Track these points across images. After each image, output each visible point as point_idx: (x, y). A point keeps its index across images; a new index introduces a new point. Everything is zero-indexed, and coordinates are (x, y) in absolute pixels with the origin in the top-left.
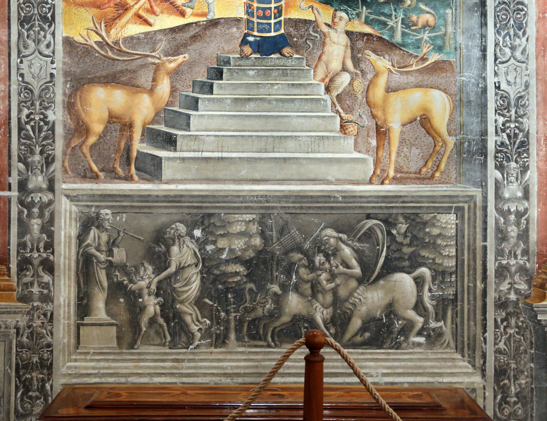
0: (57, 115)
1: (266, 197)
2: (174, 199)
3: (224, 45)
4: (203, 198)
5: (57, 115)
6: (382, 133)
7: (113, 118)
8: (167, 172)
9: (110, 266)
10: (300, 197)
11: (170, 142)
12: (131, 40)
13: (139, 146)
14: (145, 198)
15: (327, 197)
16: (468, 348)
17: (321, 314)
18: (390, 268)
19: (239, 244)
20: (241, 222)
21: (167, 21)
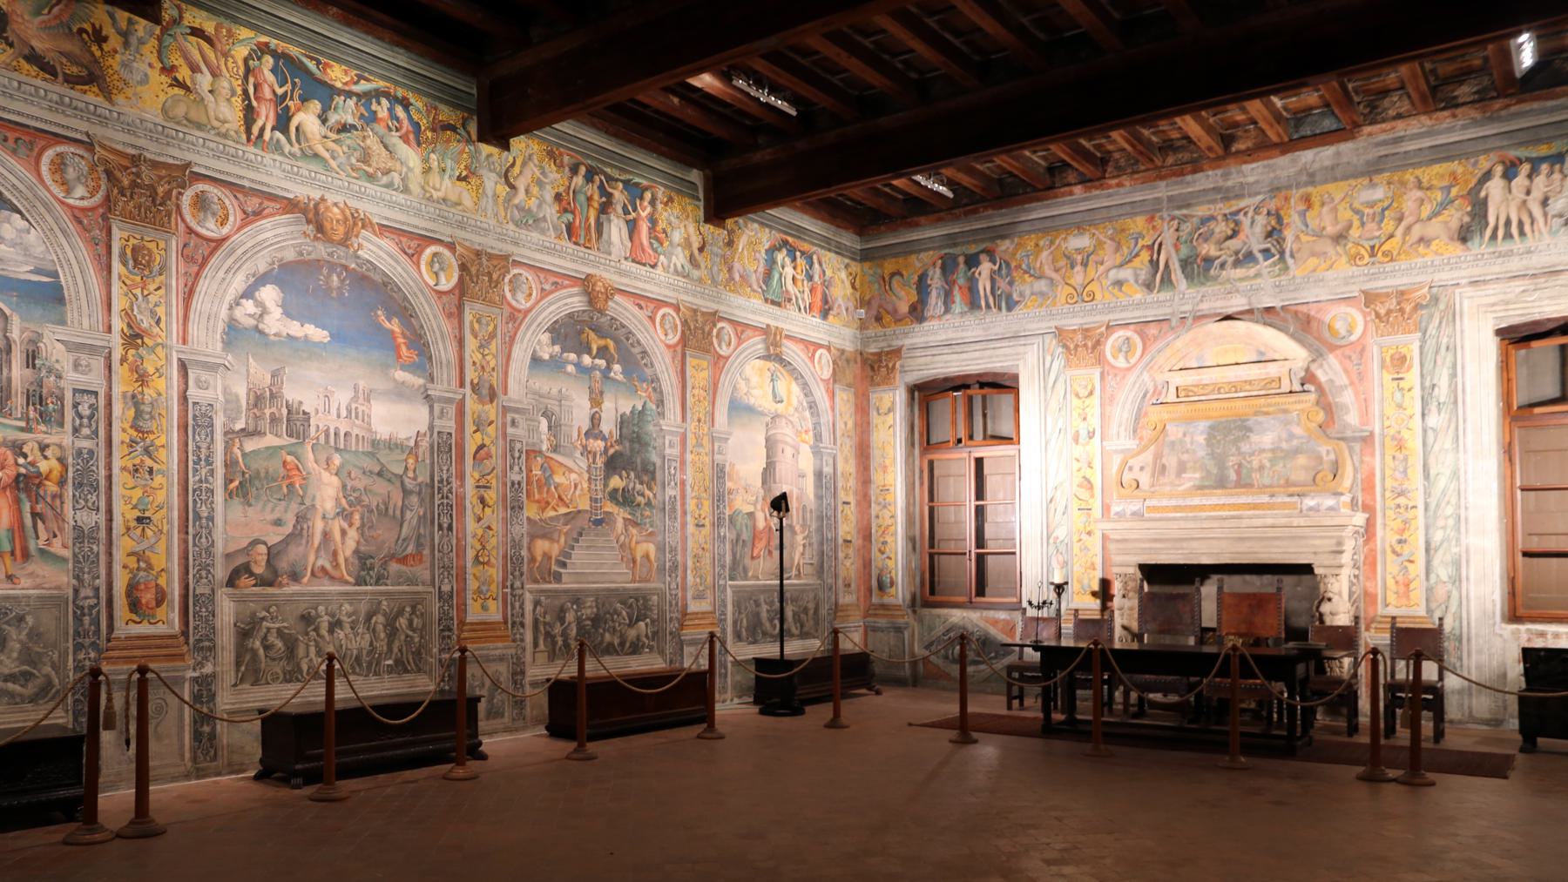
0: (524, 553)
1: (597, 590)
2: (566, 591)
3: (582, 522)
4: (577, 591)
5: (524, 553)
6: (634, 561)
7: (545, 554)
8: (564, 578)
9: (545, 624)
10: (608, 590)
11: (564, 565)
12: (551, 519)
13: (554, 568)
14: (556, 591)
15: (617, 589)
16: (662, 652)
17: (616, 642)
18: (638, 620)
19: (589, 611)
20: (590, 601)
21: (563, 510)
